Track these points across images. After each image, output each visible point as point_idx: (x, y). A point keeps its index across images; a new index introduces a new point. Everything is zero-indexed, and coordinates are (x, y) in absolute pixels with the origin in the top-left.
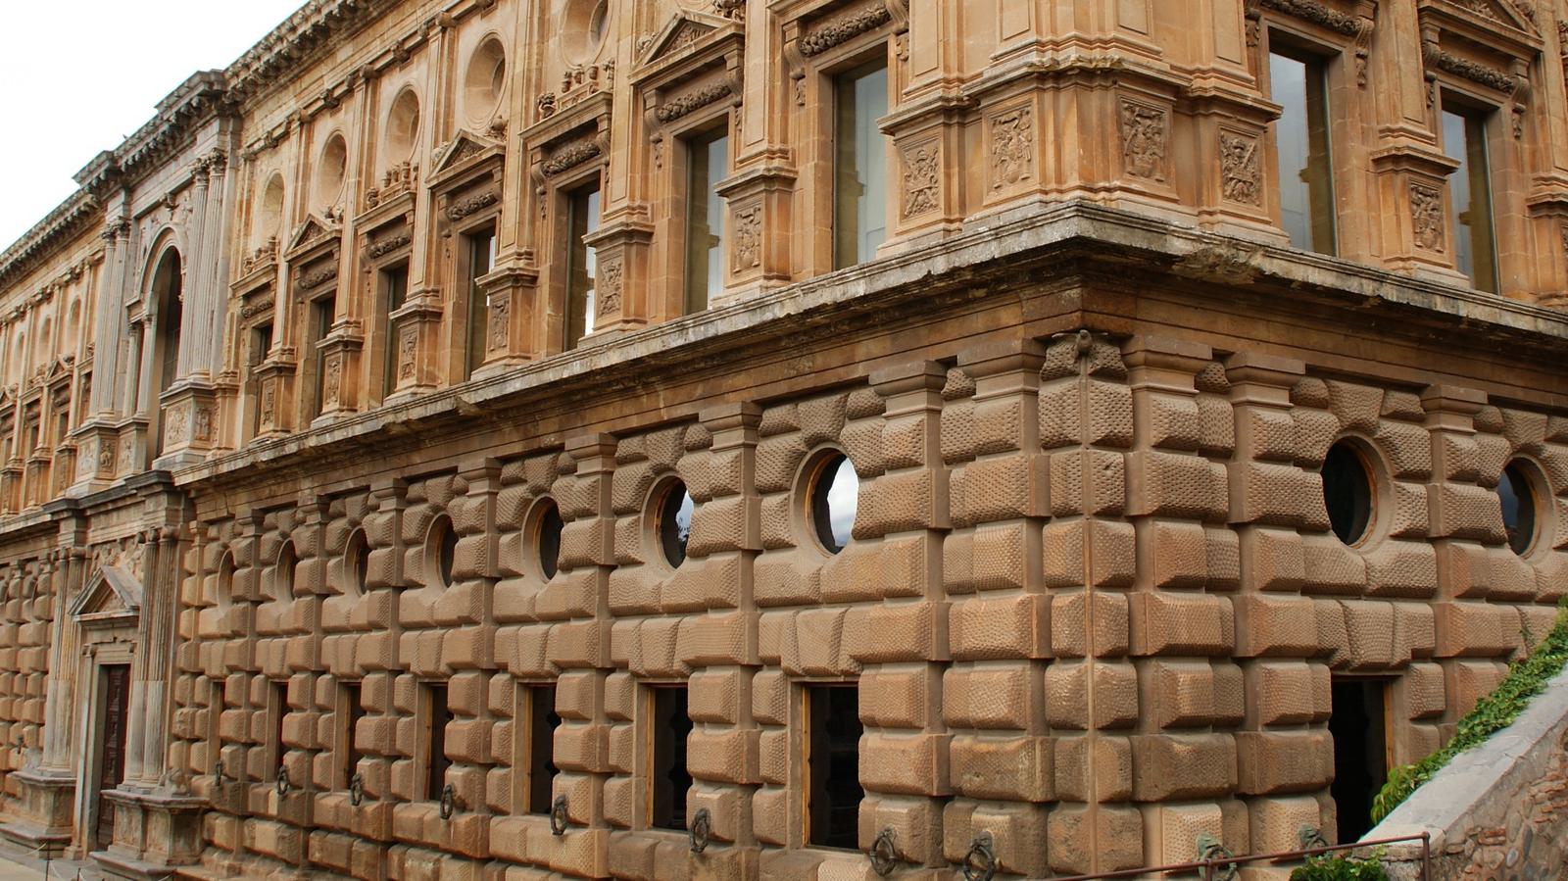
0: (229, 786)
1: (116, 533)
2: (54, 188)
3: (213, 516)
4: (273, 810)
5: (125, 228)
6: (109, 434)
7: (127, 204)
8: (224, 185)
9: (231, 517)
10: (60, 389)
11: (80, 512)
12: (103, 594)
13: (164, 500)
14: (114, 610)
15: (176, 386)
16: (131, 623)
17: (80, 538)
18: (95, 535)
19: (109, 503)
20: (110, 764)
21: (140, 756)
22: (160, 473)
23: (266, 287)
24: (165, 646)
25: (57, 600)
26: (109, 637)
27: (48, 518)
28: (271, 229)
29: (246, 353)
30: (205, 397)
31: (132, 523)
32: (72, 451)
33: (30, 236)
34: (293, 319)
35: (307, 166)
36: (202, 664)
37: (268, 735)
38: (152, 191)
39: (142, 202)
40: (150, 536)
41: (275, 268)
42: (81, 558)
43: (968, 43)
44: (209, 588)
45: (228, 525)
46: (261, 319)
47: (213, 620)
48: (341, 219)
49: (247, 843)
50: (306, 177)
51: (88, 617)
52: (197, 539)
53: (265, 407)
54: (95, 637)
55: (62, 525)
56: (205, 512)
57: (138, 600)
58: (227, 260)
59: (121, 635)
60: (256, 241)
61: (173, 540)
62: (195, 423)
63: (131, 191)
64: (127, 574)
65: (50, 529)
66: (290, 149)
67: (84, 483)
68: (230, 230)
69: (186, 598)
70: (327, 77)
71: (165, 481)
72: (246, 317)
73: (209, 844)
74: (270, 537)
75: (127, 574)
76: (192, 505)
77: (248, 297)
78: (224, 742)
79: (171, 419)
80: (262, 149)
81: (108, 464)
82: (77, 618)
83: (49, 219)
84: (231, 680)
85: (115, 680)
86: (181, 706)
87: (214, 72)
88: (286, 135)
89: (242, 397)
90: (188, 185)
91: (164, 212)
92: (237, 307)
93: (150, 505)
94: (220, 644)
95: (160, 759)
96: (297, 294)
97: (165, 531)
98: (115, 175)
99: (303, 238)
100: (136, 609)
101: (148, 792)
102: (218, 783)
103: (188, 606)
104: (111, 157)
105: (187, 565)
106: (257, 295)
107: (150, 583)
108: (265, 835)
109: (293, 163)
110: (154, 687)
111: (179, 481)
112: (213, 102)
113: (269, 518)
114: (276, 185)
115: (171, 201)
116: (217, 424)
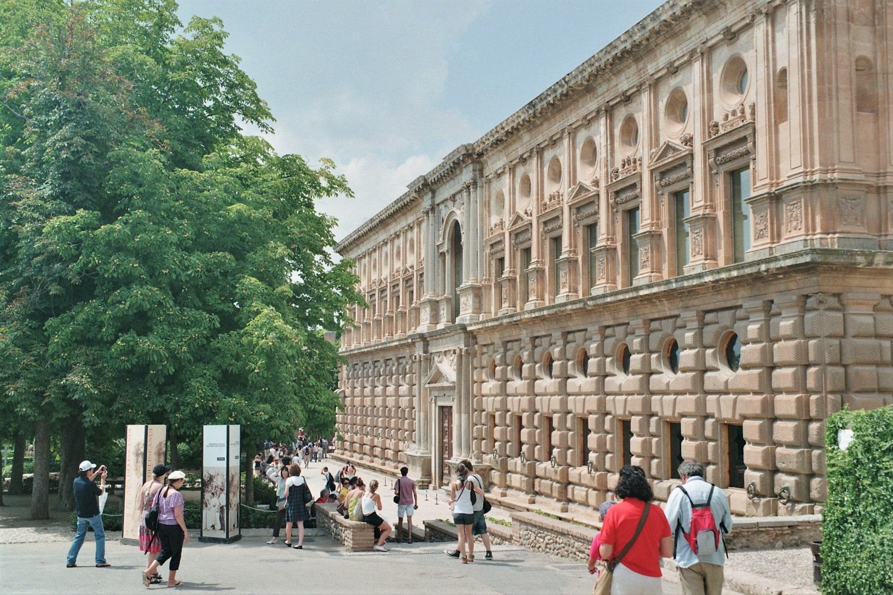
16: (452, 388)
24: (467, 399)
43: (781, 166)
45: (491, 347)
49: (508, 483)
60: (494, 220)
68: (482, 215)
73: (492, 484)
75: (448, 368)
85: (445, 412)
95: (468, 448)
100: (454, 382)
110: (464, 416)
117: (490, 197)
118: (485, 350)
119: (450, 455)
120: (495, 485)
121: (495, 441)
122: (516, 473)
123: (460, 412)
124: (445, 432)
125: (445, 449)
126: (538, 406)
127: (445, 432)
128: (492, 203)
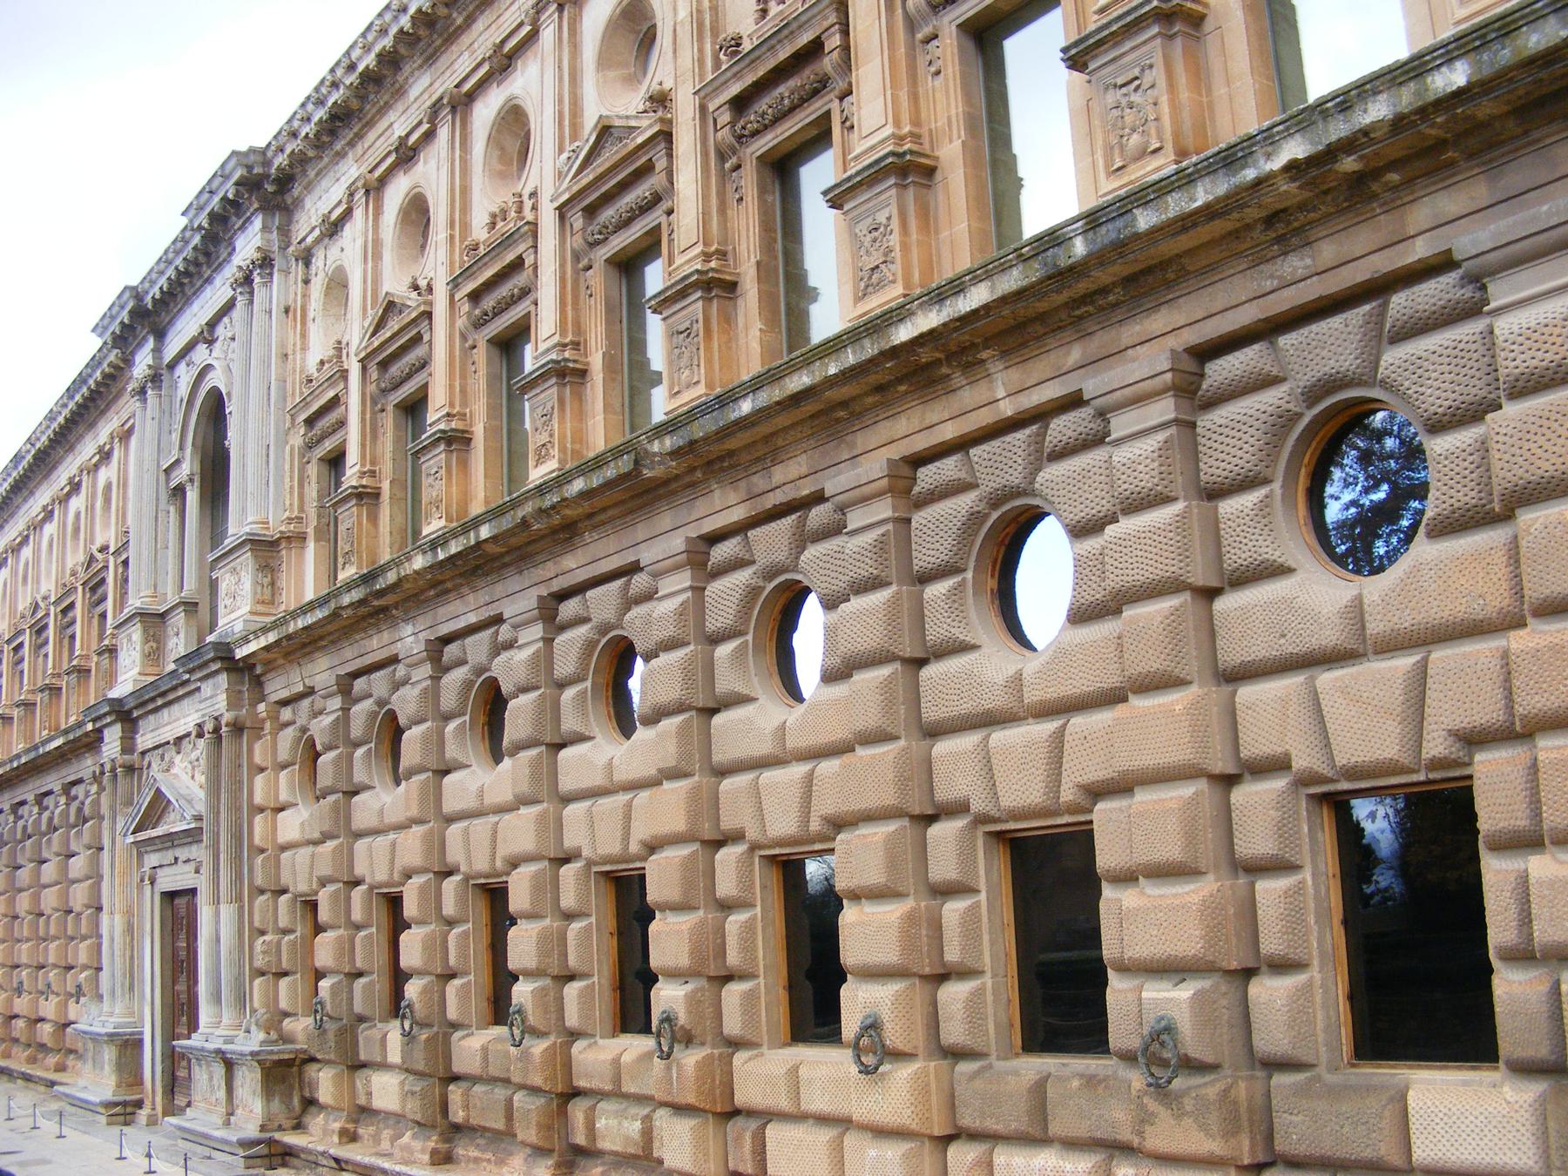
0: (331, 1027)
1: (168, 734)
3: (284, 694)
4: (395, 1056)
8: (275, 291)
9: (310, 692)
11: (127, 715)
12: (159, 806)
13: (223, 679)
14: (173, 824)
15: (229, 542)
16: (191, 836)
17: (128, 746)
18: (144, 740)
19: (155, 697)
21: (217, 998)
22: (217, 645)
23: (335, 402)
24: (237, 859)
25: (106, 824)
26: (168, 856)
27: (90, 727)
28: (338, 334)
29: (312, 492)
30: (266, 549)
31: (184, 718)
34: (371, 433)
36: (286, 879)
40: (209, 727)
41: (344, 374)
42: (130, 769)
44: (286, 785)
45: (306, 703)
46: (328, 445)
47: (291, 826)
50: (378, 256)
51: (142, 836)
52: (268, 725)
53: (343, 547)
54: (152, 859)
55: (106, 732)
56: (277, 688)
57: (201, 808)
58: (283, 381)
59: (182, 853)
60: (318, 349)
61: (238, 728)
62: (256, 583)
64: (185, 781)
65: (93, 742)
66: (354, 233)
67: (128, 678)
69: (258, 799)
70: (399, 122)
71: (225, 656)
72: (310, 446)
74: (361, 709)
75: (185, 781)
76: (258, 682)
77: (310, 422)
79: (226, 584)
80: (318, 241)
81: (154, 655)
82: (130, 839)
84: (323, 897)
85: (178, 909)
86: (263, 933)
88: (348, 214)
89: (311, 545)
92: (297, 439)
93: (207, 688)
94: (304, 853)
96: (373, 403)
97: (227, 717)
99: (380, 325)
100: (199, 818)
102: (320, 1026)
103: (262, 810)
105: (258, 759)
106: (322, 418)
107: (214, 787)
108: (385, 1090)
109: (360, 242)
110: (227, 911)
111: (240, 653)
113: (360, 684)
114: (338, 284)
116: (283, 582)
118: (286, 714)
119: (193, 1026)
120: (322, 1107)
121: (319, 975)
123: (216, 901)
124: (180, 966)
125: (181, 1011)
126: (455, 854)
127: (180, 966)
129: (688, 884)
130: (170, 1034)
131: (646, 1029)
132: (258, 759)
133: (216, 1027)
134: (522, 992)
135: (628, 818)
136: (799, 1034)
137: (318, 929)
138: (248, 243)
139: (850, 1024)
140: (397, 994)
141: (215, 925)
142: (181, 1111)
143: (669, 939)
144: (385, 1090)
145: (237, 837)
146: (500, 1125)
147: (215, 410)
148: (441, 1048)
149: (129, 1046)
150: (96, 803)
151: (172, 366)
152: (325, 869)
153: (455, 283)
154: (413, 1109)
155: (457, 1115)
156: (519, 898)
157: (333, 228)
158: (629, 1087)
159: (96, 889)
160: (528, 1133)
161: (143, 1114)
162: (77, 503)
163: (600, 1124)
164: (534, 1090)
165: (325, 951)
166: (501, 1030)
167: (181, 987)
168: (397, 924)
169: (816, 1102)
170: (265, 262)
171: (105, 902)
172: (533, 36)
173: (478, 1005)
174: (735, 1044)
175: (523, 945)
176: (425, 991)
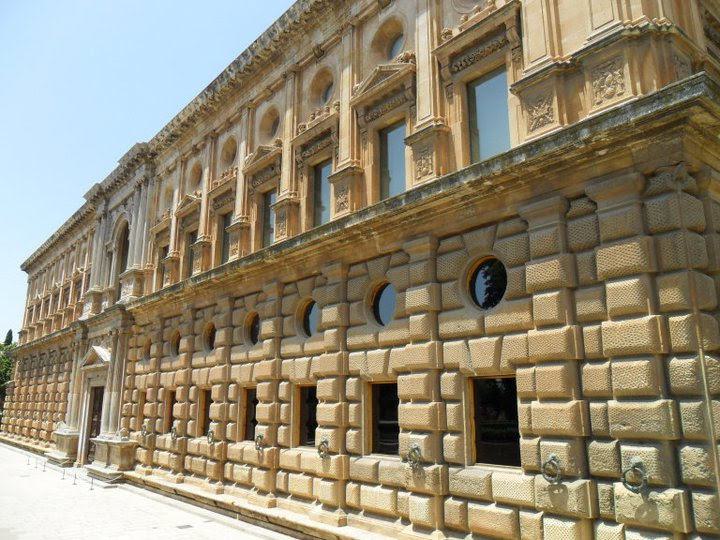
1: (99, 333)
2: (78, 202)
4: (168, 445)
5: (105, 215)
6: (98, 297)
7: (106, 205)
8: (149, 191)
10: (78, 283)
16: (105, 369)
20: (94, 428)
24: (120, 377)
32: (82, 305)
33: (66, 224)
35: (184, 178)
37: (166, 414)
38: (117, 199)
39: (112, 206)
48: (201, 196)
49: (155, 461)
50: (184, 183)
51: (87, 367)
63: (108, 201)
66: (176, 175)
67: (87, 313)
73: (137, 462)
78: (145, 417)
83: (74, 216)
86: (126, 402)
87: (144, 144)
88: (175, 169)
90: (132, 195)
91: (122, 209)
95: (116, 425)
98: (100, 194)
99: (183, 206)
101: (110, 439)
104: (99, 186)
108: (163, 457)
109: (178, 177)
110: (114, 394)
112: (143, 158)
115: (125, 203)
117: (159, 193)
119: (98, 433)
120: (140, 463)
122: (164, 450)
123: (111, 391)
125: (94, 428)
126: (195, 378)
128: (162, 198)
129: (270, 393)
130: (90, 435)
131: (253, 439)
132: (131, 344)
133: (105, 435)
134: (213, 426)
135: (252, 371)
136: (302, 443)
137: (146, 401)
138: (140, 174)
139: (318, 441)
140: (171, 424)
141: (109, 399)
142: (90, 463)
143: (262, 410)
144: (163, 457)
145: (120, 370)
146: (201, 470)
147: (126, 231)
148: (184, 444)
149: (74, 441)
150: (72, 355)
151: (110, 212)
152: (150, 381)
153: (209, 194)
154: (173, 465)
155: (187, 466)
156: (215, 394)
157: (170, 172)
158: (246, 459)
159: (67, 386)
160: (211, 473)
161: (76, 463)
162: (73, 254)
163: (235, 471)
164: (214, 460)
165: (147, 408)
166: (204, 438)
167: (95, 419)
168: (173, 400)
169: (306, 466)
170: (146, 181)
171: (70, 389)
172: (240, 117)
173: (198, 430)
174: (280, 446)
175: (215, 409)
176: (180, 425)
